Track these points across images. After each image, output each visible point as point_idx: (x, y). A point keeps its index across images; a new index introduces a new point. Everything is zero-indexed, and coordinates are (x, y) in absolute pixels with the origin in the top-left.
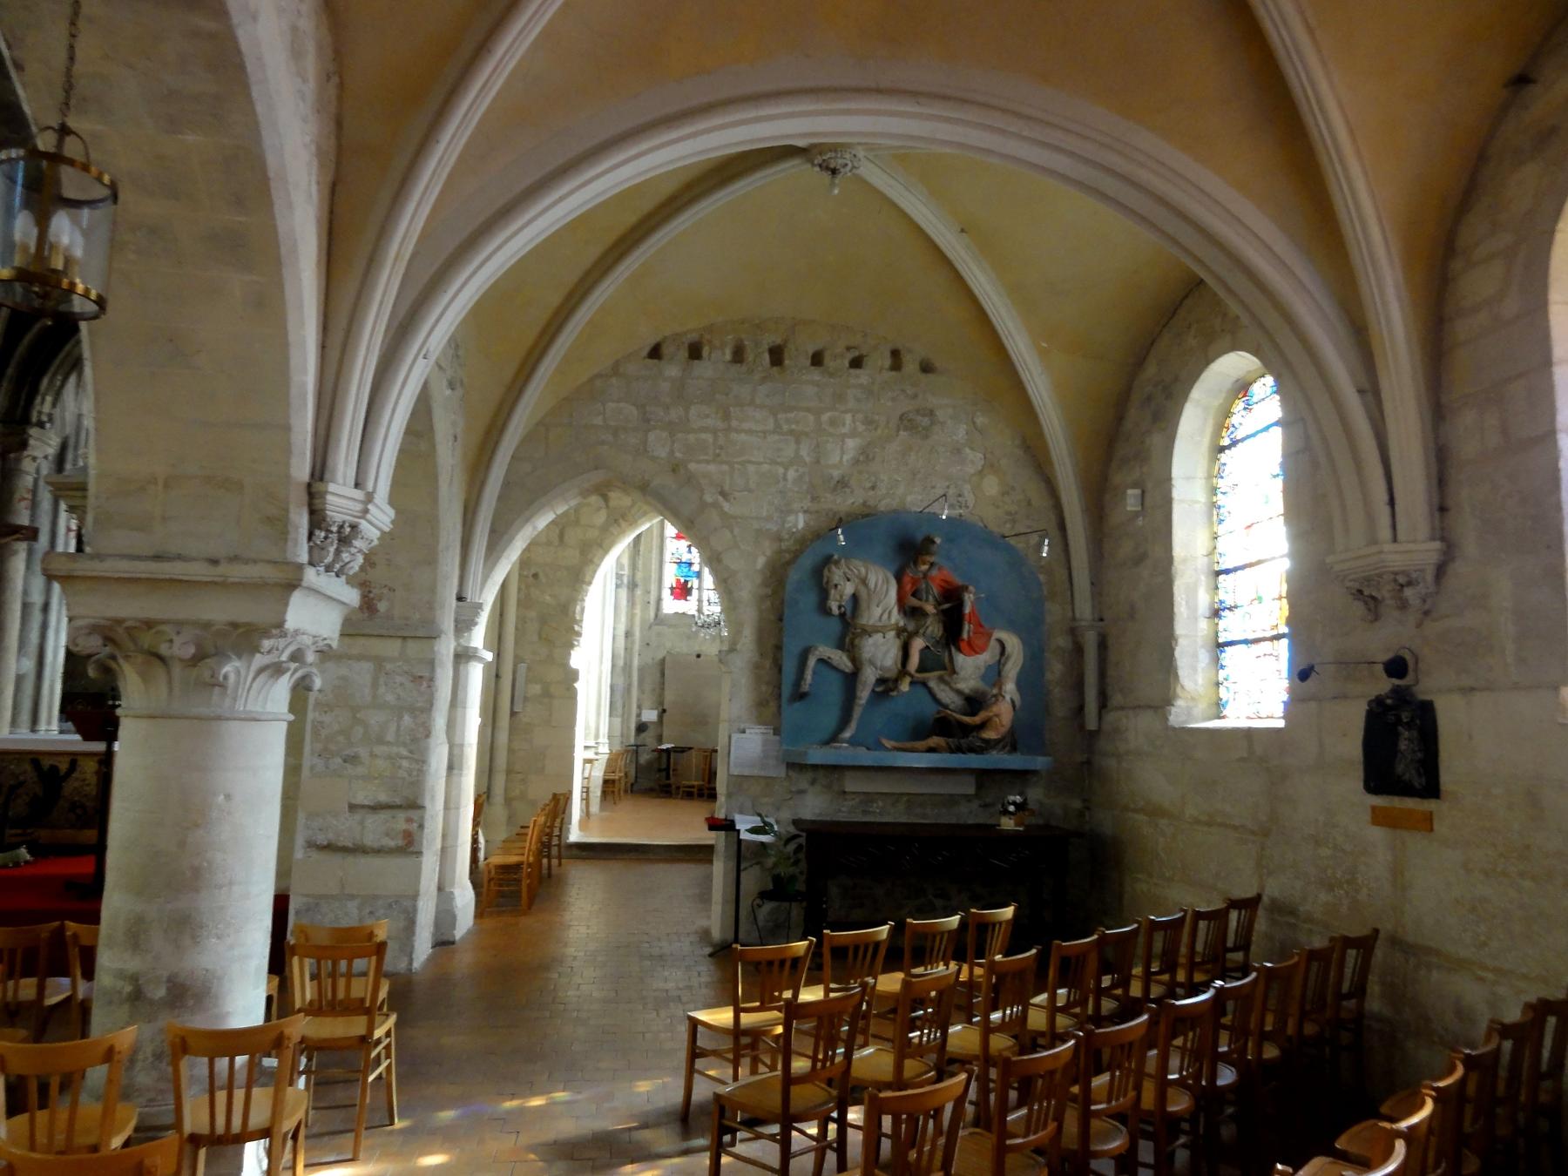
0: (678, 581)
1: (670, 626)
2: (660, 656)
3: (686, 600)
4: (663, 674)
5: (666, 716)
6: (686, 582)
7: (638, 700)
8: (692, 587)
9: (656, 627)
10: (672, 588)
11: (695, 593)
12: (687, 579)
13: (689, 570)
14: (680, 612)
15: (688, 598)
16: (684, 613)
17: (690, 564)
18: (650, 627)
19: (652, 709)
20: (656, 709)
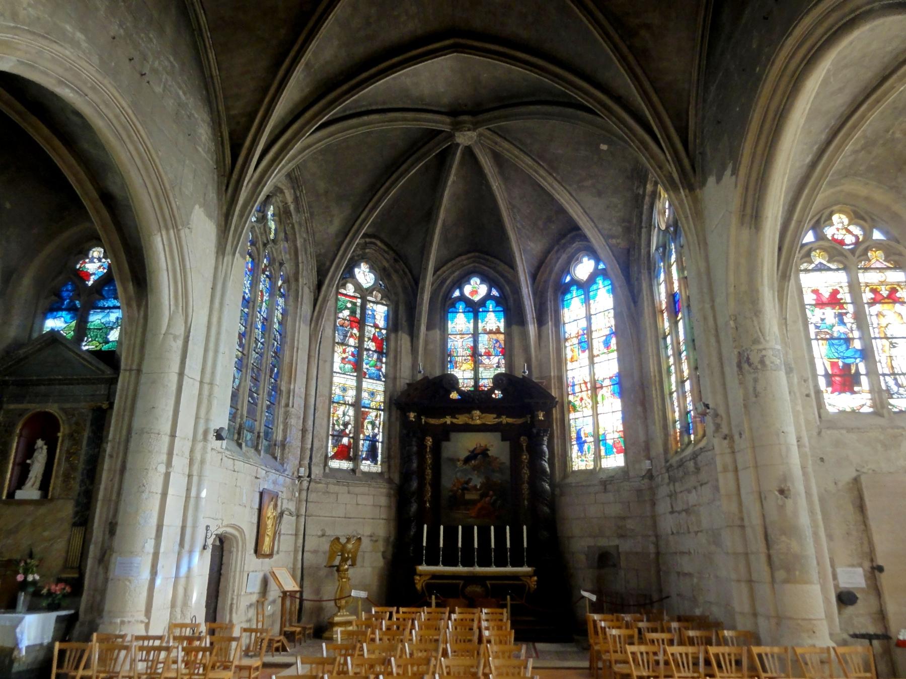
0: (834, 365)
1: (850, 430)
2: (847, 475)
3: (853, 392)
4: (861, 508)
5: (884, 579)
6: (847, 366)
7: (829, 550)
8: (858, 373)
9: (829, 432)
10: (827, 375)
11: (864, 380)
12: (848, 361)
13: (848, 348)
14: (848, 410)
15: (856, 389)
16: (853, 411)
17: (848, 341)
18: (819, 433)
19: (853, 566)
20: (860, 565)
